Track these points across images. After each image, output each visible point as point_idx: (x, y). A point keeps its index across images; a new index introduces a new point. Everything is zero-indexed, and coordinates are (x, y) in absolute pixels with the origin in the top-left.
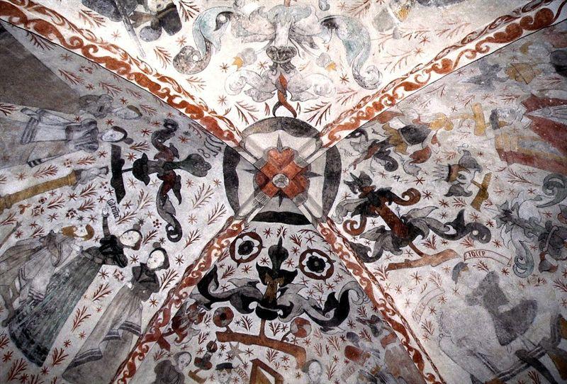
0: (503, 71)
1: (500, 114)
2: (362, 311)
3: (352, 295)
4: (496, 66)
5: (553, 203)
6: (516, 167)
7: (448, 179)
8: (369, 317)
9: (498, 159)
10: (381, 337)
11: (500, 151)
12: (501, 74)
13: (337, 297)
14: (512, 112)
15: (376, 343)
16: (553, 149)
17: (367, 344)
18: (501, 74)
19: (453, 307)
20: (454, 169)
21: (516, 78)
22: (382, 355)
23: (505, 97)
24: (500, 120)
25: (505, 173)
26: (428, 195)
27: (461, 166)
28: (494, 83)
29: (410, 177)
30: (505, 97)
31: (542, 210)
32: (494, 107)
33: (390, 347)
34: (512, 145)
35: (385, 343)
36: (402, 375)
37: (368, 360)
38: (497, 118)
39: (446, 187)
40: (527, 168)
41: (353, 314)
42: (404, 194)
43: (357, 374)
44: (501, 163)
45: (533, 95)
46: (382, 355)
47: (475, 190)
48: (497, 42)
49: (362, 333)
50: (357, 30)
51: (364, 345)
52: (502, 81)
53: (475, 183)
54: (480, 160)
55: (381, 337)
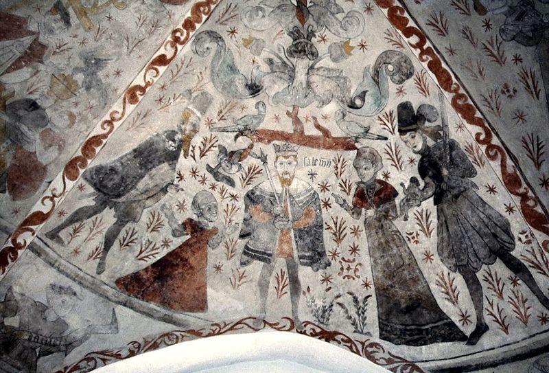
0: (80, 83)
1: (61, 24)
4: (88, 88)
14: (51, 31)
18: (79, 77)
21: (65, 79)
23: (66, 47)
24: (59, 16)
28: (82, 65)
30: (66, 47)
32: (71, 29)
38: (62, 18)
48: (97, 136)
52: (77, 69)
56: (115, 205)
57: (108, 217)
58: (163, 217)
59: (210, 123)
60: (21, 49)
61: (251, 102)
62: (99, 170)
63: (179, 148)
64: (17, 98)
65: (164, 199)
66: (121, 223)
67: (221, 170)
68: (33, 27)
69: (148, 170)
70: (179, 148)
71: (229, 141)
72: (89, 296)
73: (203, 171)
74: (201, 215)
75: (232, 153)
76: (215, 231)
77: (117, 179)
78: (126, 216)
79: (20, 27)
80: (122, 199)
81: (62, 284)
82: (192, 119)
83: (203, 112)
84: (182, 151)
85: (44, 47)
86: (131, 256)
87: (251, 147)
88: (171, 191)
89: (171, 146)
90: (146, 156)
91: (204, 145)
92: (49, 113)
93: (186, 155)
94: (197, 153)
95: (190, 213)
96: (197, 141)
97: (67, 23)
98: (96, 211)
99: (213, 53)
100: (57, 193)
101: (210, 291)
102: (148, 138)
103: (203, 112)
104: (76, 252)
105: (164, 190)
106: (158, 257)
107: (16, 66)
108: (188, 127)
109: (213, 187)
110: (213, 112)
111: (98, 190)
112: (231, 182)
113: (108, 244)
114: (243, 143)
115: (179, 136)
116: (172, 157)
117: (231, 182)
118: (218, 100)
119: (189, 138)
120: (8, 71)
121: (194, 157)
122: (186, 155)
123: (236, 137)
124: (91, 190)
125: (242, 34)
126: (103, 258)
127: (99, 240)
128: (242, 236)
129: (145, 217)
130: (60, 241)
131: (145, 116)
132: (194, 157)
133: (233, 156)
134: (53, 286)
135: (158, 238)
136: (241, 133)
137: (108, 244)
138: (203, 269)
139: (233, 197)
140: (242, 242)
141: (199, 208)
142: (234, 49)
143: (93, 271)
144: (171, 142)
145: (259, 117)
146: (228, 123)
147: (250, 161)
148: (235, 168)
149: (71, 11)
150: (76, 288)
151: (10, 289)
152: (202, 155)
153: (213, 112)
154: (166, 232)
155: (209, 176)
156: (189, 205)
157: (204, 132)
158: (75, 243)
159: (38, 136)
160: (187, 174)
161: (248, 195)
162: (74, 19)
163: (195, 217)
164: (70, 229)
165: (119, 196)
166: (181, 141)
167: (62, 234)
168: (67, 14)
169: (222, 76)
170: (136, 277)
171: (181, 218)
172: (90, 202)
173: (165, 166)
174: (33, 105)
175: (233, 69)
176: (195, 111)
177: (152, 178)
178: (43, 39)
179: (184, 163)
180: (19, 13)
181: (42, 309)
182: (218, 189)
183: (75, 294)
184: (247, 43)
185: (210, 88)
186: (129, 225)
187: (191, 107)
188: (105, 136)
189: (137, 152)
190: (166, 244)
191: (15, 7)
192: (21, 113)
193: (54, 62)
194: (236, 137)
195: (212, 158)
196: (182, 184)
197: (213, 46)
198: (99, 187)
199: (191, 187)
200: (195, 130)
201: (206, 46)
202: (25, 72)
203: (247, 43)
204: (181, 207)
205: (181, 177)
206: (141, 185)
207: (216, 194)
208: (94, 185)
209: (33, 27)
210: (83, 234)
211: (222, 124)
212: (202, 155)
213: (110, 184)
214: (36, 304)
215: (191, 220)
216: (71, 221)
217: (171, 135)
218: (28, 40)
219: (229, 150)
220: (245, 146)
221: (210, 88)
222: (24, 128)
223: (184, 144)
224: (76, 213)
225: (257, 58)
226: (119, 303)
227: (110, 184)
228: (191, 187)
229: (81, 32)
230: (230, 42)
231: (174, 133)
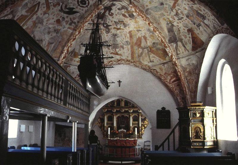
2: (74, 19)
3: (78, 14)
5: (123, 44)
6: (128, 35)
7: (119, 21)
8: (74, 21)
9: (128, 31)
10: (70, 27)
11: (131, 31)
12: (151, 34)
13: (74, 10)
15: (68, 26)
16: (135, 41)
17: (65, 24)
19: (87, 35)
20: (123, 22)
22: (65, 29)
25: (126, 33)
26: (113, 17)
27: (124, 24)
29: (117, 13)
31: (121, 42)
33: (69, 30)
34: (133, 34)
35: (69, 28)
36: (63, 36)
37: (60, 26)
39: (117, 21)
40: (129, 37)
41: (71, 16)
42: (112, 13)
43: (54, 26)
44: (128, 32)
45: (147, 38)
46: (65, 29)
47: (119, 27)
49: (67, 21)
50: (160, 9)
51: (64, 23)
52: (150, 33)
53: (120, 27)
54: (127, 28)
55: (70, 27)
56: (178, 41)
57: (179, 43)
58: (185, 34)
59: (168, 15)
60: (144, 39)
61: (165, 6)
62: (169, 40)
63: (171, 23)
64: (152, 45)
65: (181, 31)
66: (182, 42)
67: (179, 18)
68: (140, 36)
69: (173, 31)
70: (171, 23)
71: (173, 13)
72: (192, 56)
73: (178, 21)
74: (187, 27)
75: (176, 14)
76: (191, 28)
77: (172, 38)
78: (181, 40)
79: (140, 38)
80: (177, 39)
81: (187, 58)
82: (166, 18)
83: (165, 16)
84: (172, 23)
85: (144, 36)
86: (189, 45)
87: (176, 10)
88: (180, 29)
89: (170, 25)
90: (170, 30)
91: (172, 18)
92: (156, 42)
93: (173, 23)
94: (174, 20)
95: (186, 29)
96: (171, 19)
97: (141, 30)
98: (177, 45)
99: (151, 11)
100: (169, 51)
101: (201, 39)
102: (166, 29)
103: (165, 16)
104: (183, 53)
105: (179, 30)
106: (191, 41)
107: (146, 42)
108: (167, 20)
109: (182, 21)
110: (165, 14)
111: (173, 43)
112: (182, 18)
113: (185, 47)
114: (174, 11)
115: (169, 23)
116: (173, 25)
117: (182, 18)
118: (162, 11)
119: (170, 20)
120: (147, 44)
121: (174, 21)
122: (173, 23)
123: (173, 11)
124: (172, 44)
125: (148, 4)
126: (187, 49)
127: (183, 48)
128: (194, 24)
129: (183, 37)
130: (179, 54)
131: (161, 28)
132: (174, 21)
133: (177, 14)
134: (186, 60)
135: (188, 38)
136: (172, 10)
137: (185, 47)
138: (197, 36)
139: (186, 19)
140: (195, 26)
141: (186, 27)
142: (151, 6)
143: (188, 53)
144: (169, 25)
145: (169, 5)
146: (169, 12)
147: (179, 12)
148: (180, 15)
149: (139, 29)
150: (189, 57)
151: (183, 66)
152: (175, 19)
153: (165, 14)
154: (188, 36)
155: (180, 21)
156: (185, 28)
157: (169, 17)
158: (181, 51)
159: (159, 46)
160: (178, 25)
161: (187, 17)
162: (141, 29)
163: (187, 29)
164: (178, 51)
165: (176, 39)
166: (170, 22)
167: (178, 53)
168: (139, 30)
169: (157, 10)
170: (193, 47)
171: (186, 31)
172: (175, 45)
173: (174, 28)
174: (154, 43)
175: (156, 7)
176: (164, 17)
177: (176, 31)
178: (143, 35)
179: (175, 24)
180: (137, 37)
181: (189, 64)
182: (183, 21)
183: (190, 58)
184: (150, 3)
185: (159, 13)
186: (183, 41)
187: (163, 18)
188: (161, 39)
189: (169, 32)
190: (190, 37)
191: (136, 38)
192: (155, 46)
193: (147, 36)
194: (173, 11)
195: (176, 18)
196: (180, 26)
197: (149, 10)
198: (173, 42)
199: (181, 25)
200: (169, 19)
201: (149, 12)
202: (148, 41)
203: (150, 3)
204: (184, 30)
205: (178, 26)
206: (176, 34)
207: (184, 22)
208: (172, 43)
209: (140, 36)
210: (180, 49)
211: (169, 13)
212: (175, 19)
213: (173, 40)
214: (188, 65)
215: (187, 30)
216: (177, 50)
217: (168, 24)
218: (142, 38)
219: (175, 14)
220: (175, 11)
221: (159, 13)
222: (157, 47)
223: (170, 22)
224: (176, 48)
225: (155, 2)
226: (195, 53)
227: (173, 40)
228: (181, 25)
229: (143, 29)
230: (149, 7)
231: (167, 23)
